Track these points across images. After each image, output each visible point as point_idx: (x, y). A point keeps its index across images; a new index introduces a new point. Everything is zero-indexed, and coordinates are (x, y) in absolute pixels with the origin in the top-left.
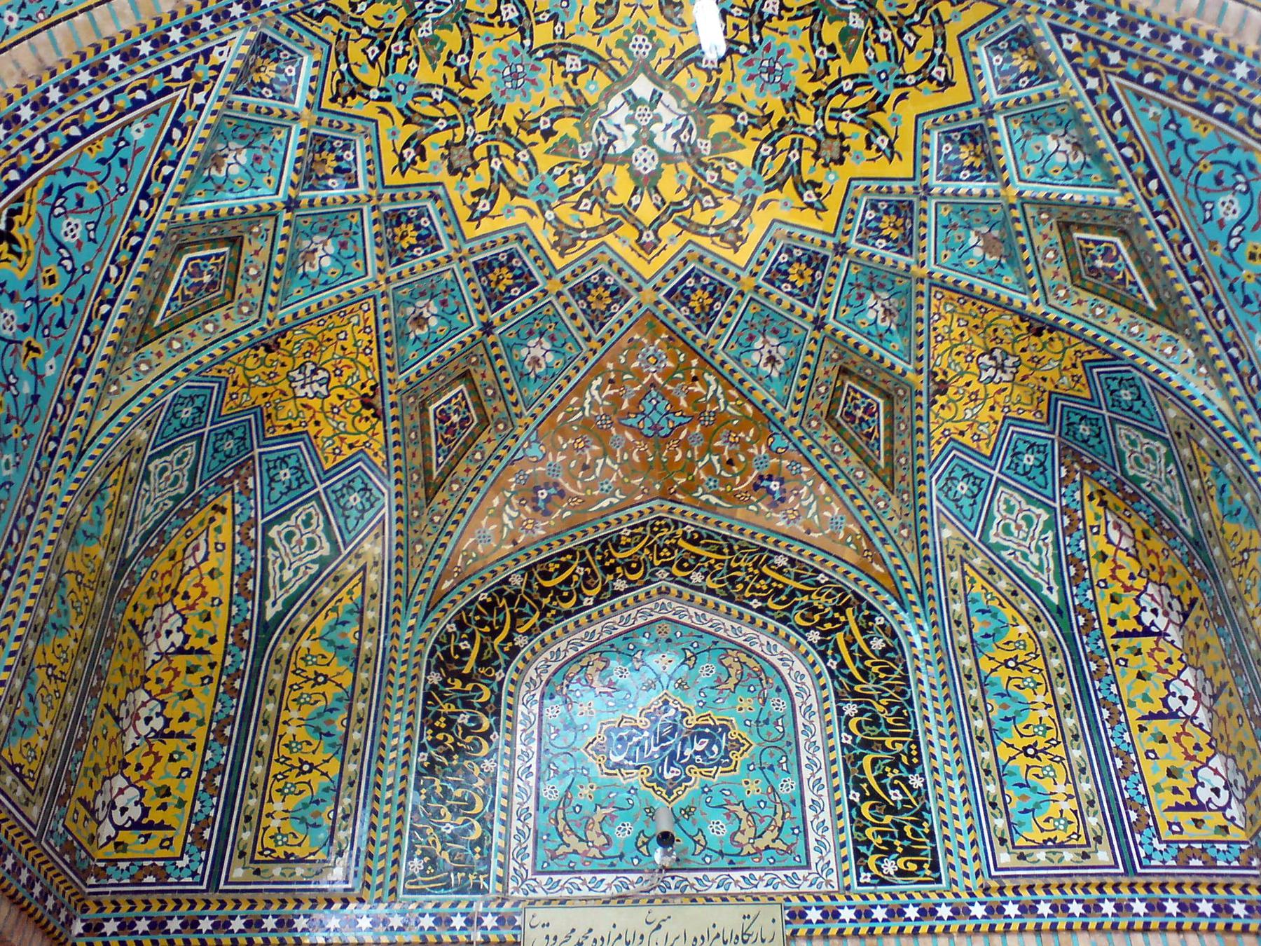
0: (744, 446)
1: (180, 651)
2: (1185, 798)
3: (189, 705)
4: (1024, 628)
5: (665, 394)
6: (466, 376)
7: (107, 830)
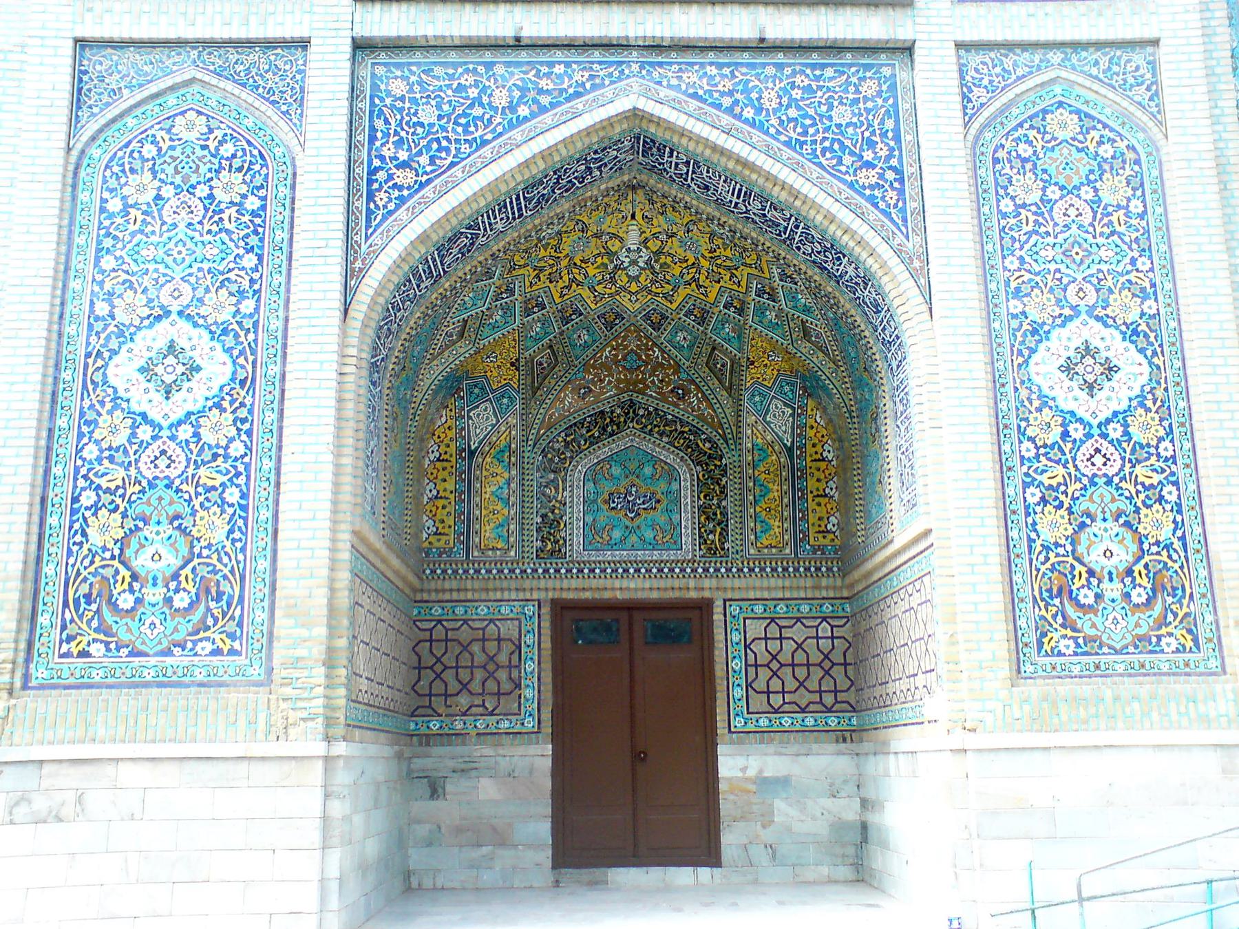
0: (668, 375)
1: (438, 460)
2: (823, 528)
3: (446, 485)
4: (774, 457)
5: (636, 354)
6: (551, 347)
7: (425, 535)
